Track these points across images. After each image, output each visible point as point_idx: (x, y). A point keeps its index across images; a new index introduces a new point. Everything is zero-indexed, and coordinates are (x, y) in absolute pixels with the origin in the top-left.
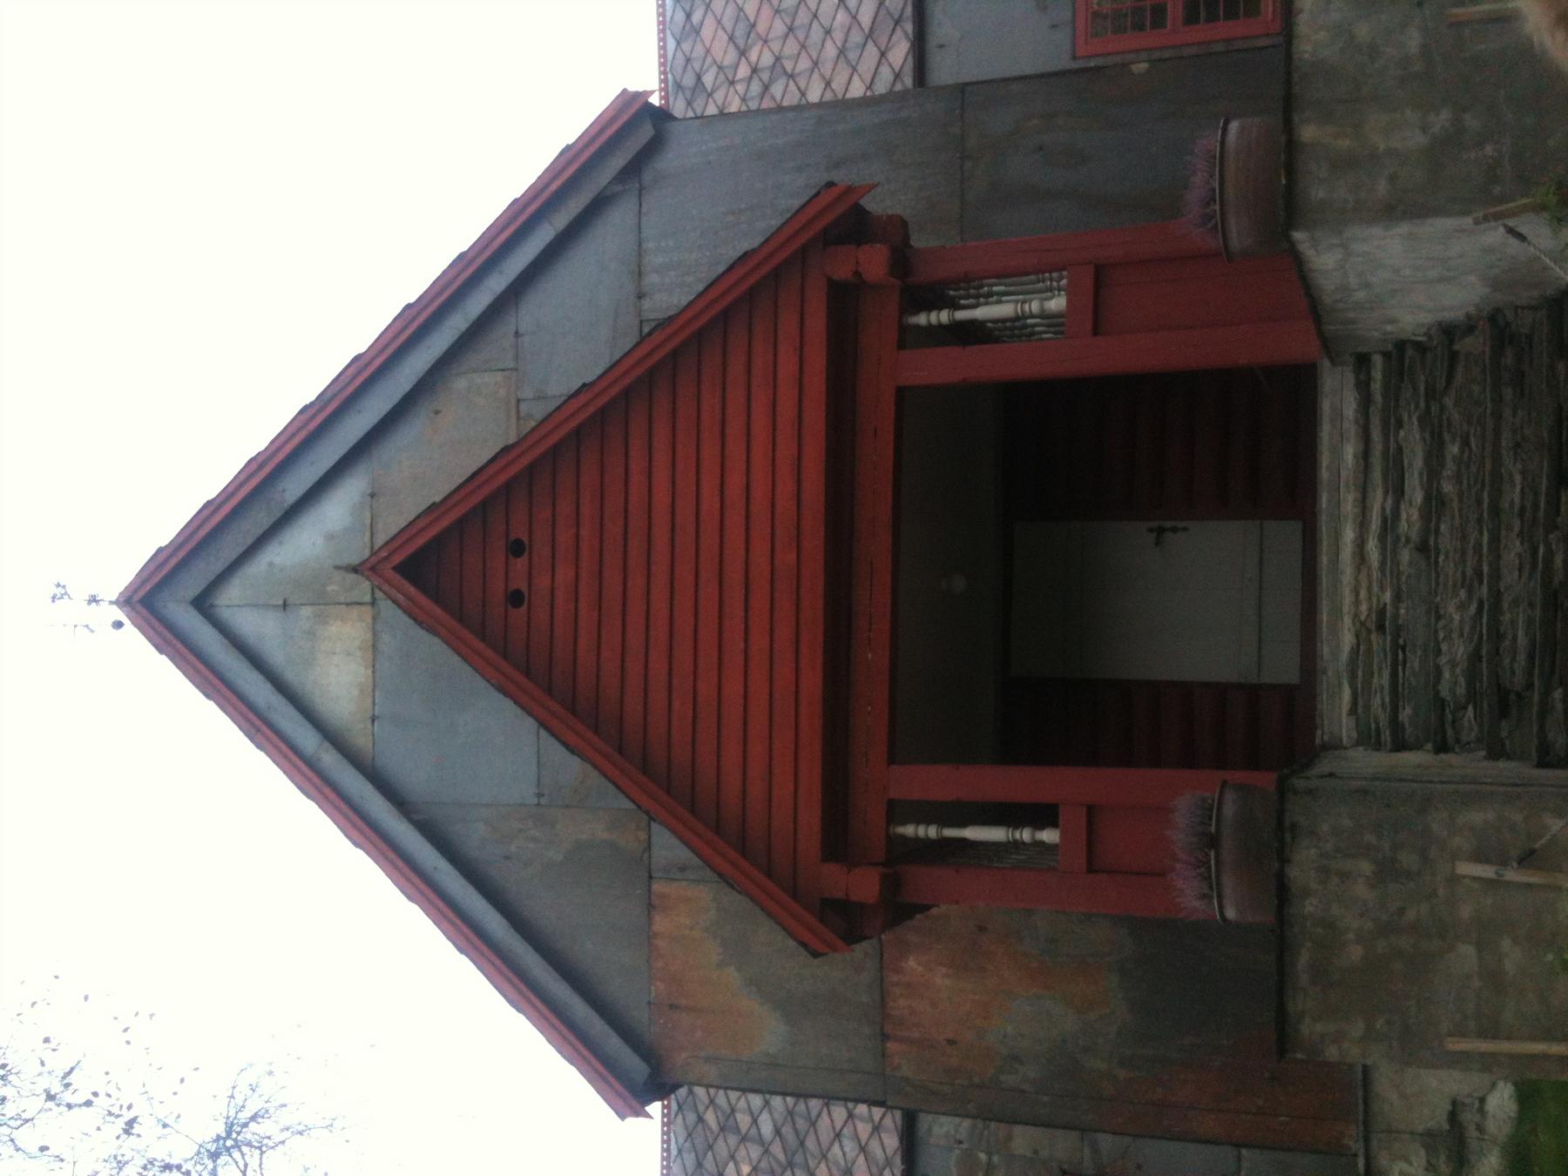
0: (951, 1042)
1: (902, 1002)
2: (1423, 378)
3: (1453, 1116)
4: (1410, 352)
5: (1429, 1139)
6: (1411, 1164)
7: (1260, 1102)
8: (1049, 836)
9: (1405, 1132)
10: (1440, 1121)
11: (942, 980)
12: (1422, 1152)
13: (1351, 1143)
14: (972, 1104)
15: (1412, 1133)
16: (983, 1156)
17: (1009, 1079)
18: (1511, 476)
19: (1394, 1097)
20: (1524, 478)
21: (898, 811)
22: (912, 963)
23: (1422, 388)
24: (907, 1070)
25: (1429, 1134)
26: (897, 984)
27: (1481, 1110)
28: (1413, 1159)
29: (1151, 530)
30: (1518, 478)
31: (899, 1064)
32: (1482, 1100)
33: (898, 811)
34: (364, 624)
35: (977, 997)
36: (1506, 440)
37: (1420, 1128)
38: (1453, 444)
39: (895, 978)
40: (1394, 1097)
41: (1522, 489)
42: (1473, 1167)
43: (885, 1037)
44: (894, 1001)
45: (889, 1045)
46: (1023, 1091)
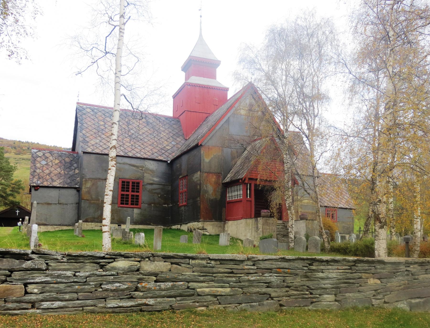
3: (205, 229)
5: (203, 227)
8: (248, 197)
10: (205, 228)
11: (213, 180)
16: (144, 169)
17: (204, 186)
21: (250, 185)
22: (215, 177)
33: (250, 185)
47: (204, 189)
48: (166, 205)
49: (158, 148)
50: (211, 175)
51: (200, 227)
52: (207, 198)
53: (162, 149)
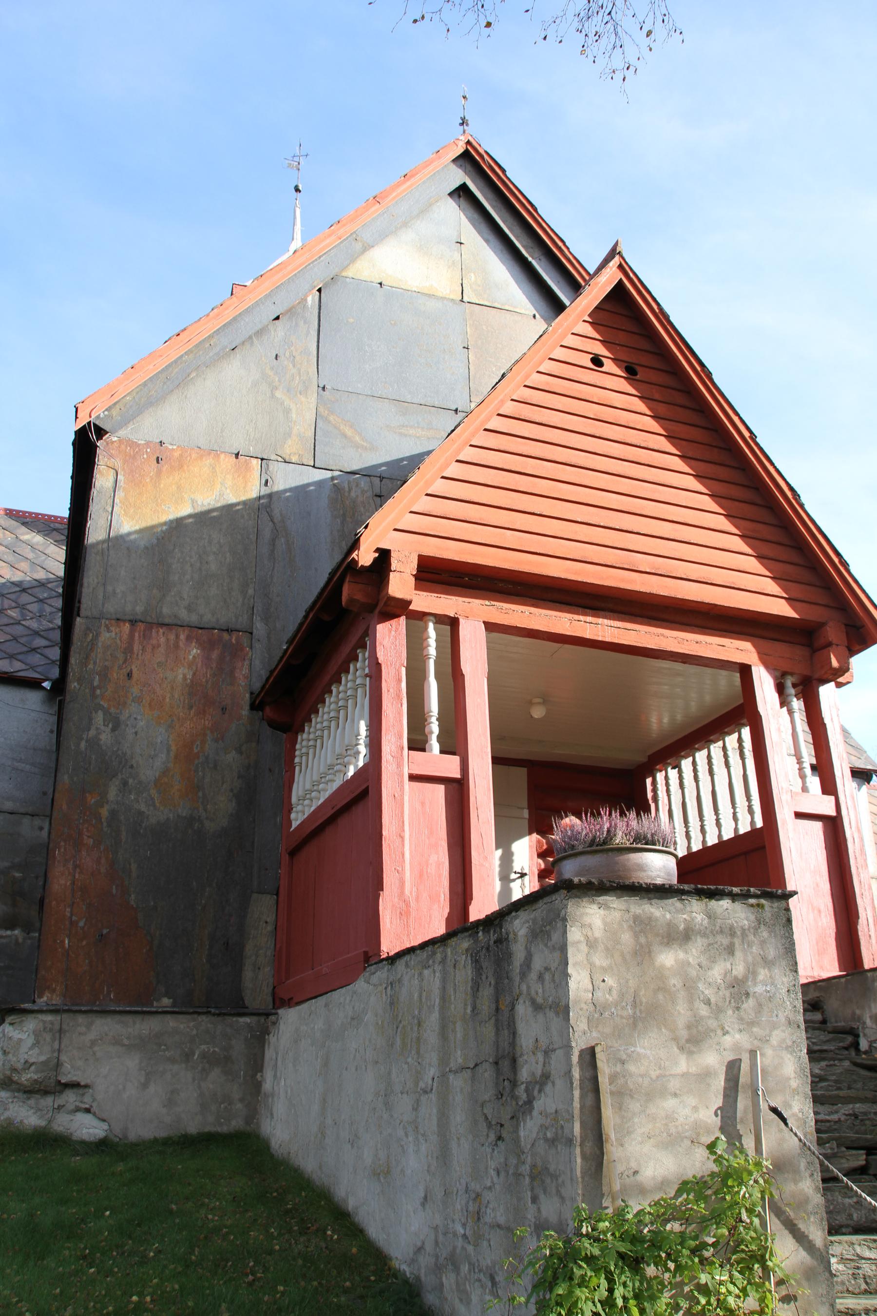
0: (129, 675)
1: (162, 640)
2: (832, 1048)
4: (850, 1039)
6: (31, 1048)
7: (81, 924)
9: (60, 1043)
11: (182, 674)
12: (43, 1058)
13: (45, 998)
14: (77, 687)
15: (59, 1051)
17: (99, 717)
18: (837, 1112)
19: (92, 1035)
20: (836, 1122)
23: (825, 1048)
24: (105, 636)
25: (58, 1065)
26: (177, 636)
27: (77, 1110)
28: (36, 1051)
29: (522, 868)
30: (835, 1117)
31: (112, 631)
32: (88, 1111)
34: (448, 292)
35: (168, 700)
36: (859, 1107)
37: (63, 1058)
38: (820, 1069)
39: (182, 637)
40: (92, 1035)
41: (828, 1121)
42: (24, 1102)
43: (133, 622)
44: (164, 633)
45: (127, 625)
46: (89, 730)
47: (94, 743)
48: (16, 932)
49: (18, 630)
50: (161, 637)
51: (28, 1065)
52: (113, 813)
53: (36, 633)
